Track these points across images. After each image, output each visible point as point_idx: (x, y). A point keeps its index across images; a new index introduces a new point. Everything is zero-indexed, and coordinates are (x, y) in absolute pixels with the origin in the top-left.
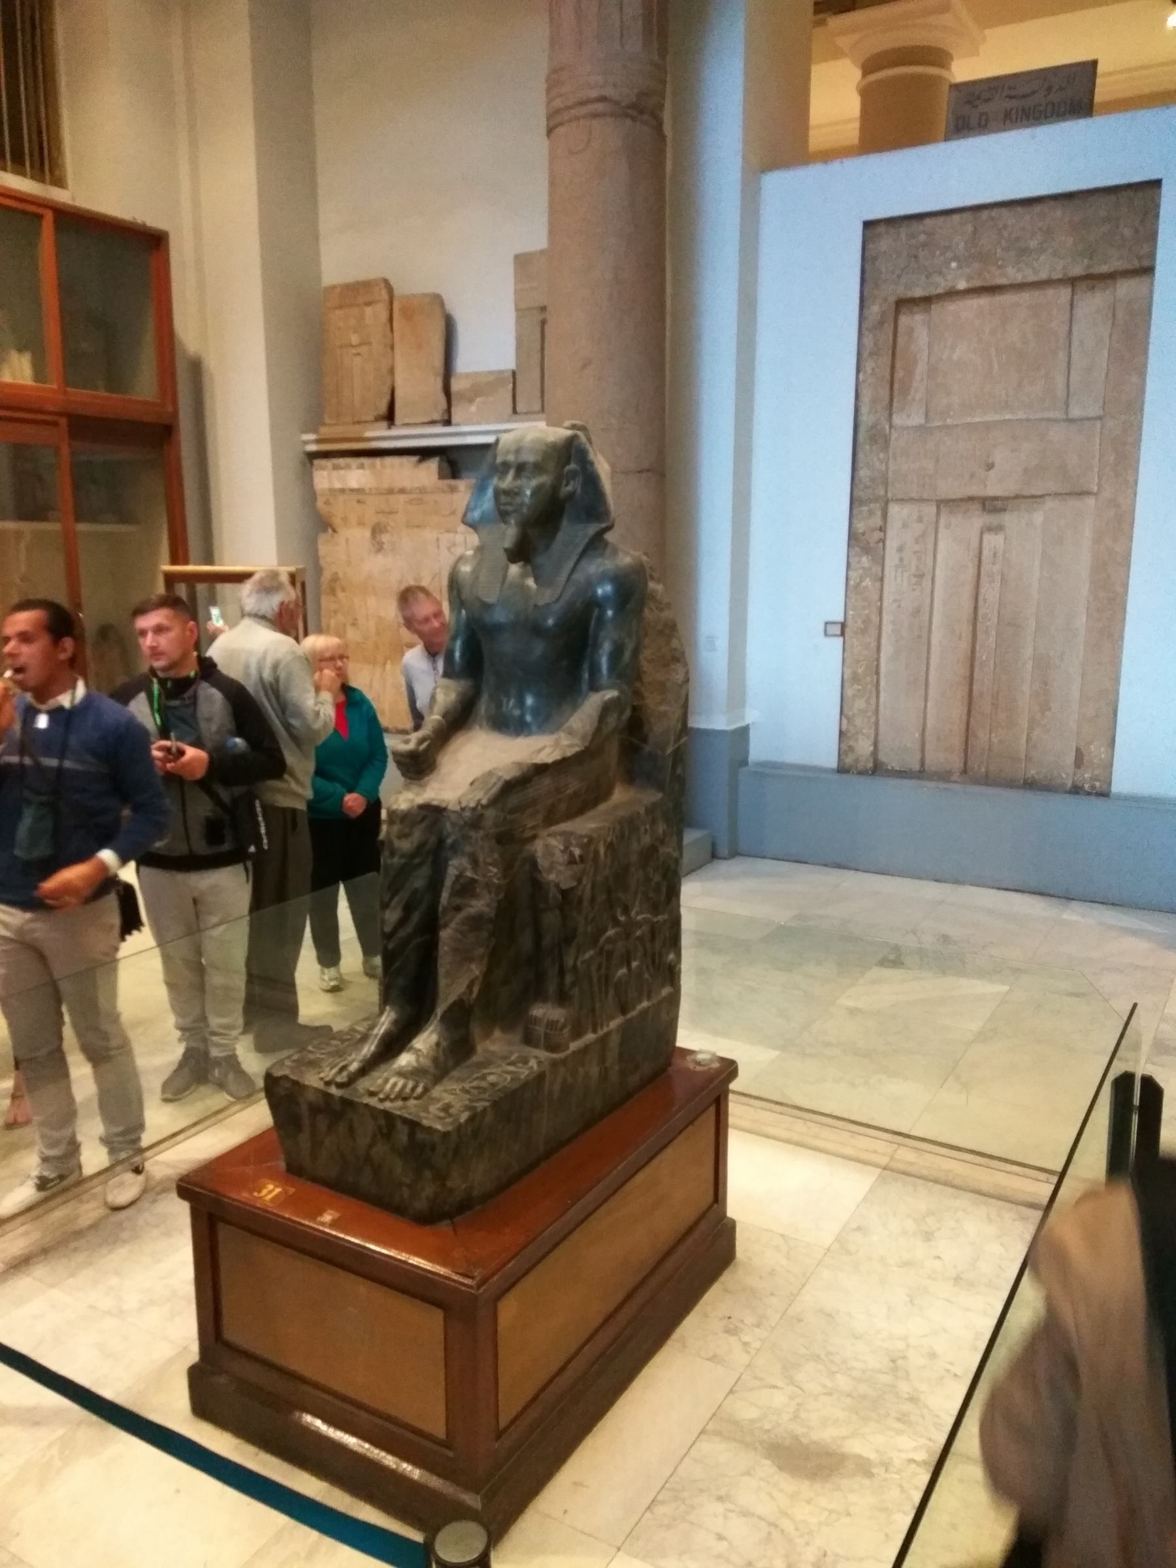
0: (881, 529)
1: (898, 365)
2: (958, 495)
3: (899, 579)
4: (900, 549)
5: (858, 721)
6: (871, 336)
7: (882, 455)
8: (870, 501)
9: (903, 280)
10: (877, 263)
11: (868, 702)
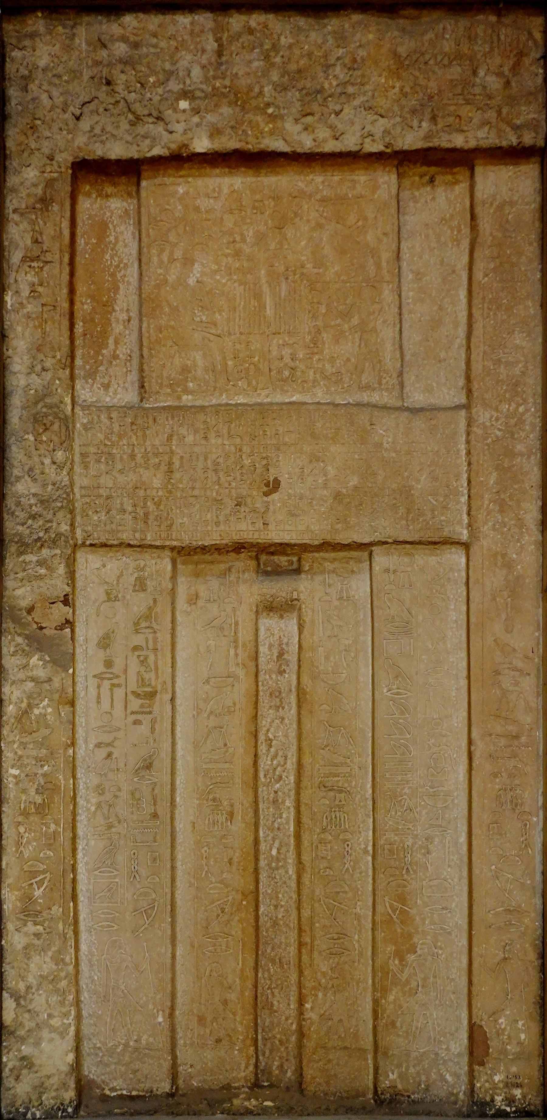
0: (66, 602)
1: (81, 288)
2: (214, 537)
3: (106, 705)
4: (105, 642)
5: (39, 1001)
6: (24, 225)
7: (60, 455)
8: (41, 543)
9: (85, 125)
10: (33, 87)
11: (58, 960)
